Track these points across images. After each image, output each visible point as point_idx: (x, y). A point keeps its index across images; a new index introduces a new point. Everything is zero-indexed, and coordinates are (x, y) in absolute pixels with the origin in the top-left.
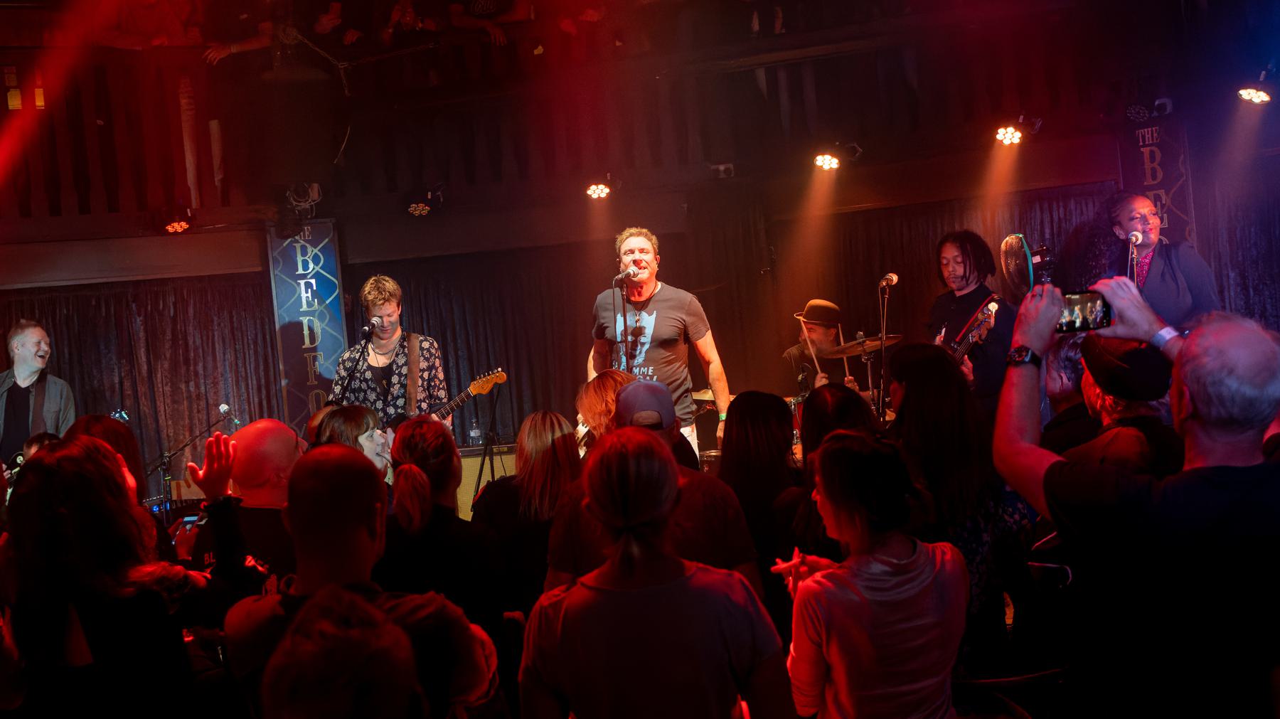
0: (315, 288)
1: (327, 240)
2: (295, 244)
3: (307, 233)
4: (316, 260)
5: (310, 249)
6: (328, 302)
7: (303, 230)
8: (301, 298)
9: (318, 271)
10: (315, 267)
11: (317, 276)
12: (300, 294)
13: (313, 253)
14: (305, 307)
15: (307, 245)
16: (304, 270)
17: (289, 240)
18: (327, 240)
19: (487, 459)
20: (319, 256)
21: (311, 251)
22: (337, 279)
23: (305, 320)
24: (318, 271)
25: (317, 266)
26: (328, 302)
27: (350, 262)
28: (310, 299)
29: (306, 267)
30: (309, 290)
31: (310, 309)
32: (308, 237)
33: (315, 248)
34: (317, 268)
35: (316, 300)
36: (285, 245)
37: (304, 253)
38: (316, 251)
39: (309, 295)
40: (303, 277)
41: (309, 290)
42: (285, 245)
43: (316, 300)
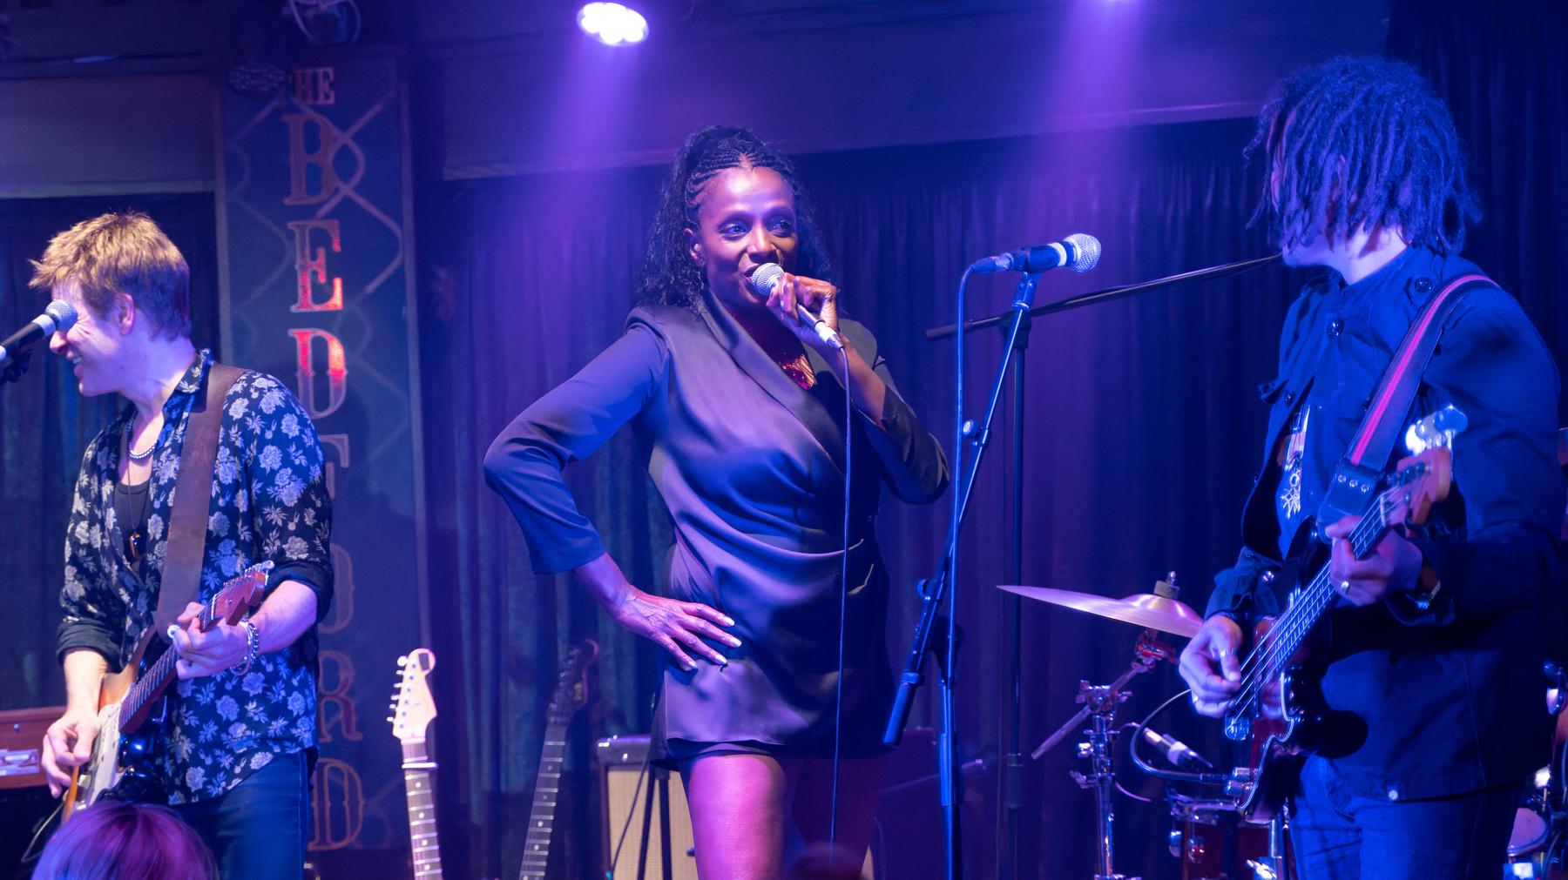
0: (337, 248)
1: (377, 109)
2: (285, 118)
3: (324, 86)
4: (344, 164)
5: (329, 129)
6: (371, 288)
7: (315, 77)
8: (291, 273)
9: (347, 200)
10: (340, 184)
11: (346, 211)
12: (293, 263)
13: (338, 145)
14: (305, 304)
15: (320, 119)
16: (313, 188)
17: (274, 104)
18: (377, 109)
19: (675, 779)
20: (353, 158)
21: (337, 138)
22: (400, 221)
23: (303, 338)
24: (347, 200)
25: (346, 178)
26: (371, 288)
27: (450, 174)
28: (322, 280)
29: (313, 188)
30: (321, 252)
31: (317, 308)
32: (327, 97)
33: (344, 128)
34: (347, 190)
35: (338, 283)
36: (262, 116)
37: (313, 144)
38: (346, 139)
39: (320, 265)
40: (307, 212)
41: (321, 252)
42: (262, 116)
43: (338, 283)
